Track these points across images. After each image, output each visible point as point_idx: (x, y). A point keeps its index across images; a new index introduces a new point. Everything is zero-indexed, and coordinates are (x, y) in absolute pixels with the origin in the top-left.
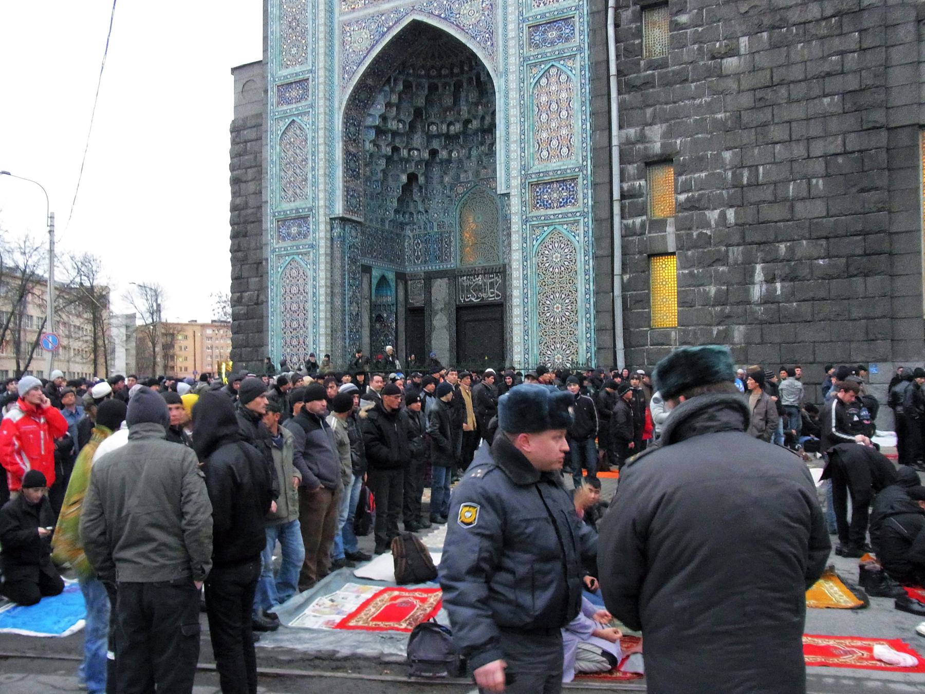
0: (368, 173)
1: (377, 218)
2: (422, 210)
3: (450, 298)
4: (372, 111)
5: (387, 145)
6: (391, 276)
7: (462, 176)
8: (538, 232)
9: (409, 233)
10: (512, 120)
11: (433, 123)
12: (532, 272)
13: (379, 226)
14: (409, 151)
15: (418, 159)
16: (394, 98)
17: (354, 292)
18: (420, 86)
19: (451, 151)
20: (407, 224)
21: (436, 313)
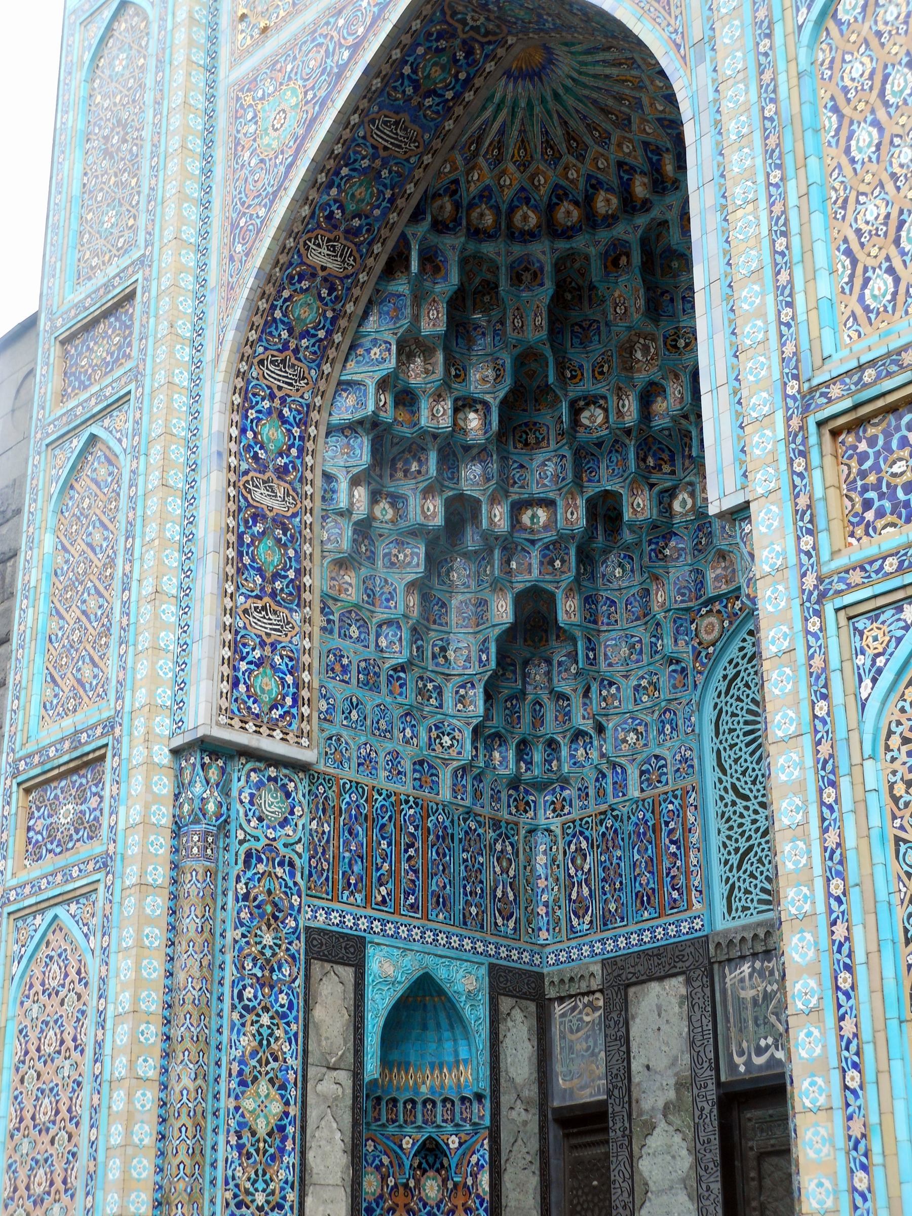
0: (353, 595)
1: (395, 756)
2: (587, 726)
3: (696, 1061)
4: (353, 370)
5: (428, 492)
6: (465, 981)
7: (710, 575)
8: (875, 634)
9: (545, 817)
10: (738, 192)
11: (591, 400)
12: (865, 834)
13: (406, 788)
14: (517, 508)
15: (549, 536)
16: (434, 322)
17: (263, 1041)
18: (523, 274)
19: (671, 493)
20: (541, 786)
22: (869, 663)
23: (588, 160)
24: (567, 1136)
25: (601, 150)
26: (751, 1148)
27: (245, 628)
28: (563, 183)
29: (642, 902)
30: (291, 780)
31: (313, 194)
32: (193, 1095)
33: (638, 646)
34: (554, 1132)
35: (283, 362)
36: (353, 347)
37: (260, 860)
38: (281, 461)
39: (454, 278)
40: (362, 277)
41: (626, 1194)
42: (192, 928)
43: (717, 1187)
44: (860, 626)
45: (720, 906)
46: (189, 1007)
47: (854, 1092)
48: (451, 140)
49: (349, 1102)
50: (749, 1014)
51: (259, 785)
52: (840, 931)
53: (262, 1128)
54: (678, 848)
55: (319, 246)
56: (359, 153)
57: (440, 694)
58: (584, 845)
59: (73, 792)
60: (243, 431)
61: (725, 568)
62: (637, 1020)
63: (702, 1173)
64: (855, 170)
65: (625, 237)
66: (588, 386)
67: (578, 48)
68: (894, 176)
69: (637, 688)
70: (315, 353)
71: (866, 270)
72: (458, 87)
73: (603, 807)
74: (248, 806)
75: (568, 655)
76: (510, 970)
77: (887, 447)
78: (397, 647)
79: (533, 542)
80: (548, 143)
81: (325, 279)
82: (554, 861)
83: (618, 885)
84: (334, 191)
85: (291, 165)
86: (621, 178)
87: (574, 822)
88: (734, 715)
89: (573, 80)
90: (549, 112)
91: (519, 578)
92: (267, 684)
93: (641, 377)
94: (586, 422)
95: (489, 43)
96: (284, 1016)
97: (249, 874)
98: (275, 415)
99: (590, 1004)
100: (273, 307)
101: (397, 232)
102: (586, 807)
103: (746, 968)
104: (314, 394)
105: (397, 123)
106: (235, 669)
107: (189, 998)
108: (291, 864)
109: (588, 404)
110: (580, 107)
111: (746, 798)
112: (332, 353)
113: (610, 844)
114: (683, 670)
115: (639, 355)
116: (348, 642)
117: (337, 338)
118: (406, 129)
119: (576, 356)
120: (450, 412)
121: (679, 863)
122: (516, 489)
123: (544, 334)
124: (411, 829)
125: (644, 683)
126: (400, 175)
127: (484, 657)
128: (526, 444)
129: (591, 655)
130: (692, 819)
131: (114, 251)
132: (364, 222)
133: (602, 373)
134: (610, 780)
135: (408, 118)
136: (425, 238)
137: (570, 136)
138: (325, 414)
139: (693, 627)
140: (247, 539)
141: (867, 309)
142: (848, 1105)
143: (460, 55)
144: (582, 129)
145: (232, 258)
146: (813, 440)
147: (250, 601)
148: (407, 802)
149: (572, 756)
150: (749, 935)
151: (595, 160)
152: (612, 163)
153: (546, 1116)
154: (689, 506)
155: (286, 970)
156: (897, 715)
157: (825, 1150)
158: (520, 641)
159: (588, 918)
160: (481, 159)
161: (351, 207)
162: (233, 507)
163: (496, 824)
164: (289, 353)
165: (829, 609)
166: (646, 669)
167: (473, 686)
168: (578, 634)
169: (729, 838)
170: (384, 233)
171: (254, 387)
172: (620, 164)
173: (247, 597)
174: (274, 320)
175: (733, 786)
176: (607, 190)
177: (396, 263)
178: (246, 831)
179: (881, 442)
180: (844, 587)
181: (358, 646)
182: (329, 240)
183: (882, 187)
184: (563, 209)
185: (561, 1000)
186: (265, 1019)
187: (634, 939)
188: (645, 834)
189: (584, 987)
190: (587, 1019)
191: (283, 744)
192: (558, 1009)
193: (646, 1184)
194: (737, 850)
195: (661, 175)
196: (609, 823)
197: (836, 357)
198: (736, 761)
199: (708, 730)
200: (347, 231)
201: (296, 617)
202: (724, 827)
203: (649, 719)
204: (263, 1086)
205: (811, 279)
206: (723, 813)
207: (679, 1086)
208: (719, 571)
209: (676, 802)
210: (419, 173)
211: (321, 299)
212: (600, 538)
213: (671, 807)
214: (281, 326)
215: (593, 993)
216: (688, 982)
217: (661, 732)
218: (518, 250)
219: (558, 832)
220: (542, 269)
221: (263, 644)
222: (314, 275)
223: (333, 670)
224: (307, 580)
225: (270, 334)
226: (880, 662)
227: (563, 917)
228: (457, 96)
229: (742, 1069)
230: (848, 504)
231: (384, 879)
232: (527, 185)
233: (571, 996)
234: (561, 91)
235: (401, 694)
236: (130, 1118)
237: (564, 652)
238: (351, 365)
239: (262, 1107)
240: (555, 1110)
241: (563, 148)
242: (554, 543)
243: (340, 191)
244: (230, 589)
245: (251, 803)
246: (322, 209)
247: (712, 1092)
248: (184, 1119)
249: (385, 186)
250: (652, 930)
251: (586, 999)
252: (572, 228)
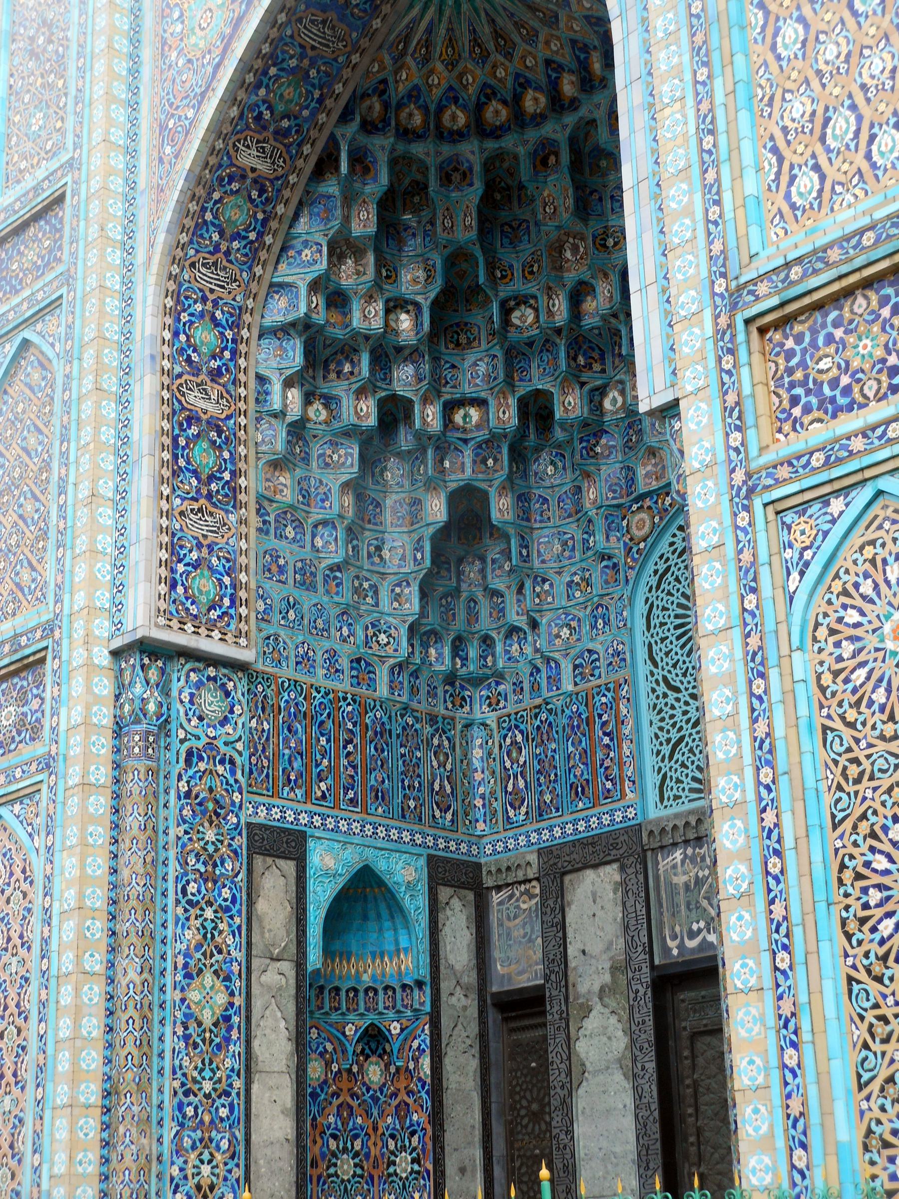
0: (288, 496)
1: (332, 654)
2: (521, 622)
3: (630, 945)
4: (285, 272)
5: (361, 393)
6: (405, 872)
7: (641, 472)
8: (803, 528)
9: (481, 712)
10: (665, 90)
11: (522, 300)
12: (793, 723)
13: (343, 685)
14: (449, 408)
16: (364, 223)
17: (207, 934)
18: (453, 174)
19: (601, 391)
20: (477, 681)
21: (587, 1010)
22: (796, 556)
23: (516, 59)
24: (506, 1020)
25: (528, 48)
26: (685, 1028)
27: (182, 530)
28: (492, 82)
29: (577, 793)
30: (230, 680)
31: (241, 95)
32: (139, 988)
33: (570, 543)
34: (493, 1015)
35: (215, 264)
36: (284, 249)
37: (201, 758)
38: (214, 364)
39: (384, 178)
40: (292, 179)
41: (563, 1075)
42: (136, 826)
43: (651, 1066)
44: (788, 520)
45: (652, 795)
46: (133, 903)
47: (784, 972)
48: (379, 39)
49: (293, 991)
50: (681, 899)
51: (199, 685)
52: (770, 818)
53: (208, 1018)
54: (612, 740)
55: (248, 147)
56: (287, 52)
57: (376, 593)
58: (519, 738)
59: (15, 694)
60: (176, 334)
61: (655, 465)
62: (573, 907)
63: (638, 1053)
64: (781, 67)
65: (553, 136)
66: (518, 286)
68: (819, 73)
69: (570, 584)
70: (246, 255)
71: (792, 167)
73: (538, 701)
74: (188, 706)
75: (501, 552)
76: (447, 860)
77: (814, 344)
78: (332, 547)
79: (465, 441)
80: (476, 42)
81: (255, 181)
82: (490, 754)
83: (552, 777)
84: (262, 92)
85: (218, 66)
86: (549, 76)
87: (509, 716)
88: (664, 609)
90: (476, 10)
91: (453, 477)
92: (204, 585)
93: (571, 277)
94: (516, 321)
96: (227, 910)
97: (191, 772)
98: (207, 318)
99: (527, 892)
100: (204, 209)
101: (326, 133)
102: (521, 701)
103: (678, 855)
104: (246, 297)
105: (324, 22)
106: (173, 571)
107: (133, 894)
108: (232, 762)
109: (518, 304)
111: (677, 690)
112: (263, 255)
113: (545, 737)
114: (615, 565)
115: (568, 254)
116: (284, 543)
117: (268, 239)
118: (333, 28)
119: (507, 256)
120: (381, 313)
121: (612, 754)
122: (448, 389)
123: (473, 234)
124: (350, 726)
125: (577, 579)
126: (327, 74)
127: (419, 556)
128: (458, 344)
129: (524, 552)
130: (625, 711)
131: (43, 154)
132: (293, 123)
133: (532, 273)
134: (544, 675)
135: (335, 17)
136: (354, 139)
137: (497, 34)
138: (257, 317)
139: (625, 523)
140: (182, 442)
141: (793, 207)
142: (778, 986)
144: (510, 27)
145: (161, 161)
146: (741, 337)
147: (186, 503)
148: (345, 699)
149: (507, 652)
150: (680, 823)
151: (523, 58)
152: (540, 61)
153: (485, 1001)
154: (620, 403)
155: (229, 865)
156: (824, 608)
157: (756, 1029)
158: (454, 539)
159: (523, 810)
160: (409, 59)
161: (280, 108)
162: (167, 410)
163: (433, 719)
164: (220, 255)
165: (758, 503)
166: (578, 566)
167: (408, 584)
168: (511, 531)
169: (661, 729)
170: (313, 133)
171: (187, 290)
172: (548, 63)
173: (183, 499)
174: (205, 222)
175: (665, 678)
176: (536, 89)
177: (325, 165)
178: (186, 730)
179: (807, 339)
180: (772, 482)
181: (295, 547)
182: (258, 142)
183: (808, 84)
184: (491, 109)
185: (499, 888)
186: (209, 913)
187: (569, 828)
188: (579, 727)
189: (520, 875)
190: (524, 906)
191: (221, 643)
192: (496, 898)
193: (583, 1065)
194: (668, 741)
195: (589, 73)
196: (544, 716)
197: (763, 255)
198: (667, 654)
199: (640, 624)
200: (276, 133)
201: (233, 518)
202: (656, 719)
203: (581, 614)
204: (208, 978)
205: (738, 176)
206: (655, 706)
207: (614, 970)
208: (649, 468)
209: (609, 695)
210: (346, 73)
211: (252, 201)
212: (532, 436)
213: (604, 700)
214: (212, 229)
215: (530, 881)
216: (622, 869)
217: (594, 626)
218: (447, 150)
219: (494, 726)
220: (471, 169)
221: (199, 546)
222: (244, 177)
223: (269, 570)
224: (242, 482)
225: (201, 236)
226: (808, 555)
227: (499, 809)
229: (675, 952)
230: (776, 400)
231: (323, 775)
232: (456, 86)
233: (508, 885)
235: (337, 593)
236: (78, 1012)
237: (498, 549)
238: (283, 267)
239: (208, 998)
240: (494, 995)
241: (491, 46)
242: (487, 442)
243: (268, 93)
244: (167, 492)
245: (191, 702)
246: (251, 110)
247: (646, 975)
248: (131, 1011)
249: (313, 86)
250: (587, 820)
251: (523, 888)
252: (501, 127)
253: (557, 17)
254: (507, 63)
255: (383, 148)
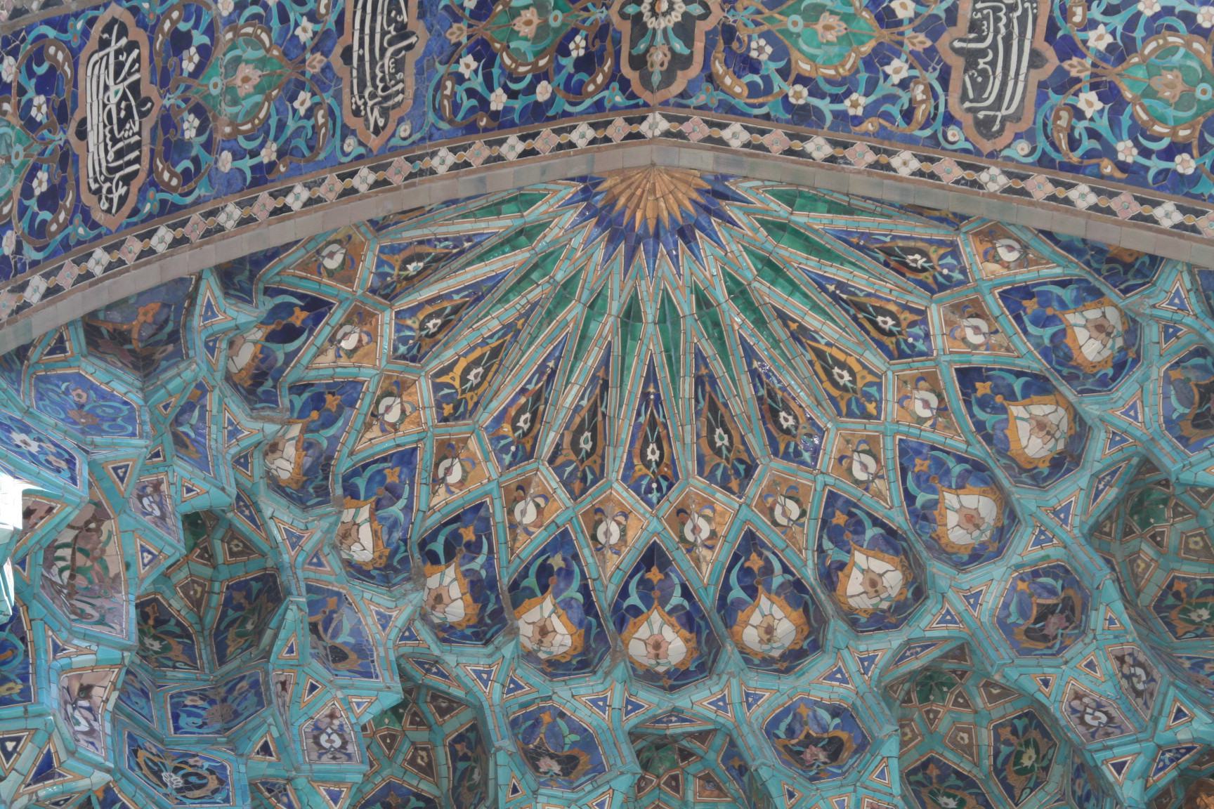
23: (587, 503)
28: (498, 513)
40: (99, 259)
65: (585, 716)
67: (817, 221)
72: (518, 104)
80: (536, 402)
86: (624, 594)
89: (703, 302)
95: (625, 85)
110: (663, 374)
118: (399, 65)
137: (592, 421)
143: (578, 48)
172: (653, 557)
210: (331, 185)
228: (501, 121)
234: (650, 312)
253: (750, 469)
254: (562, 495)
255: (234, 433)
